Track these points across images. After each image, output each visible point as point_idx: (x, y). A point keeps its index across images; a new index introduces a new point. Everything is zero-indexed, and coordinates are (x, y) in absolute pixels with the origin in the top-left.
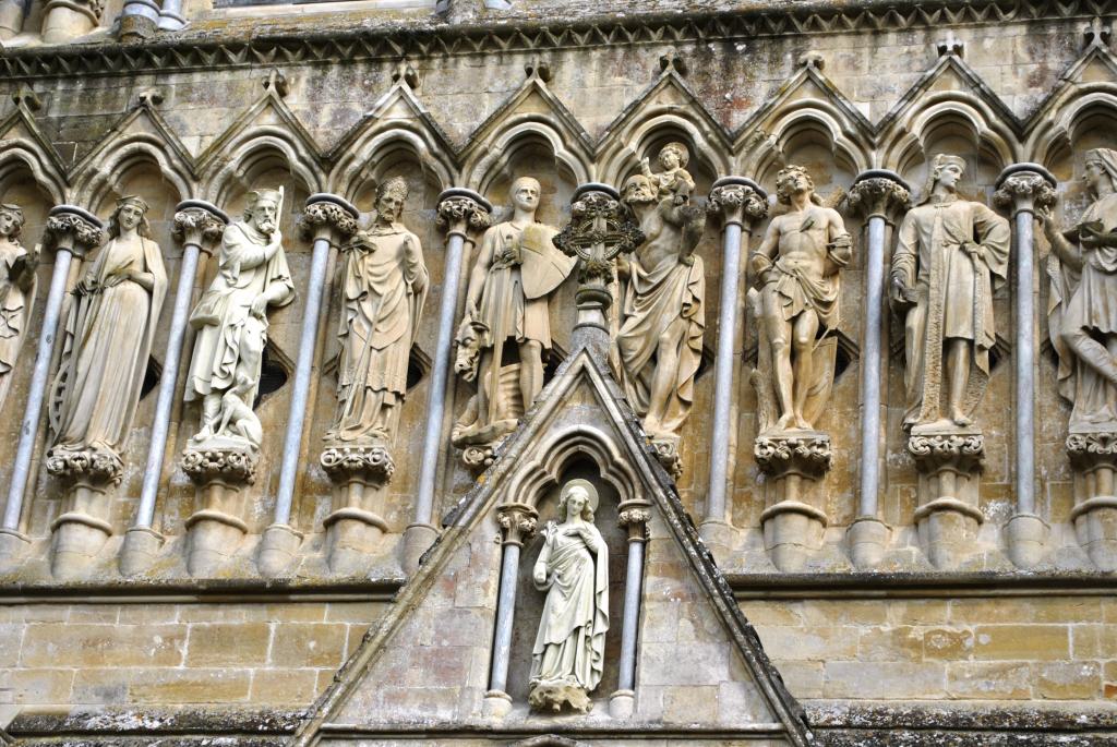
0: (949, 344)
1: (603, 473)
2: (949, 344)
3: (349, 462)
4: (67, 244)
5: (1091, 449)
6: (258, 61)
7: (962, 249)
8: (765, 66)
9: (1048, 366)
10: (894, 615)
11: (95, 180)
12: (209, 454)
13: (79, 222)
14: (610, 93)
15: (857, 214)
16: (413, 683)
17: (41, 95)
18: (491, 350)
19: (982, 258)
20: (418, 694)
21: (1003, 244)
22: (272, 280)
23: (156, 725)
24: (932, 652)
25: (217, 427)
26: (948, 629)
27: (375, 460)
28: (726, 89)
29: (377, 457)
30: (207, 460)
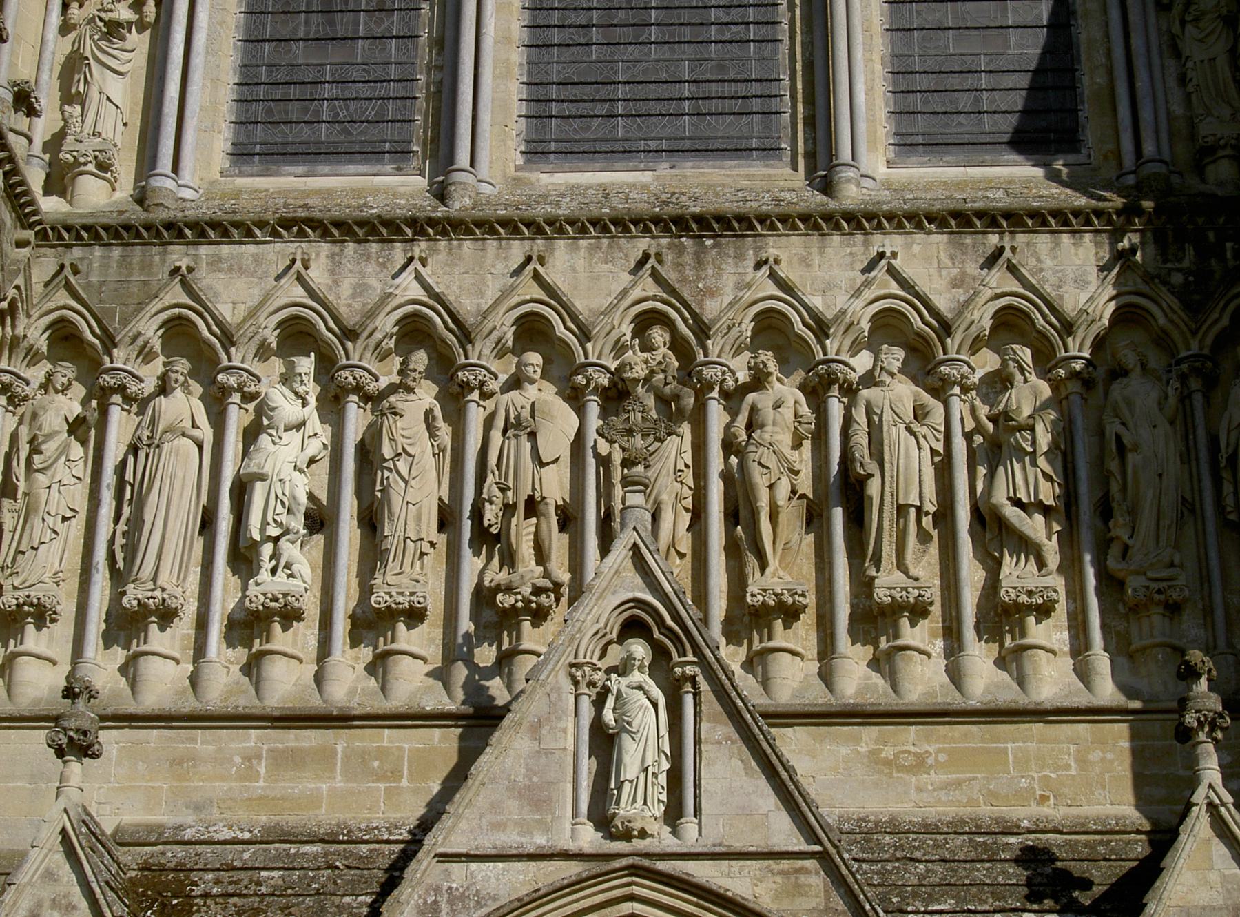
0: (902, 510)
1: (656, 634)
2: (902, 510)
3: (396, 604)
4: (117, 398)
5: (1020, 600)
6: (281, 236)
7: (908, 429)
8: (730, 260)
9: (978, 528)
10: (870, 734)
11: (140, 341)
12: (270, 595)
13: (129, 381)
14: (598, 278)
15: (816, 393)
16: (510, 813)
17: (82, 259)
18: (515, 505)
19: (924, 437)
20: (516, 823)
21: (939, 424)
22: (309, 437)
23: (247, 836)
24: (901, 769)
25: (274, 571)
26: (912, 749)
27: (419, 603)
28: (699, 279)
29: (422, 600)
30: (268, 601)
